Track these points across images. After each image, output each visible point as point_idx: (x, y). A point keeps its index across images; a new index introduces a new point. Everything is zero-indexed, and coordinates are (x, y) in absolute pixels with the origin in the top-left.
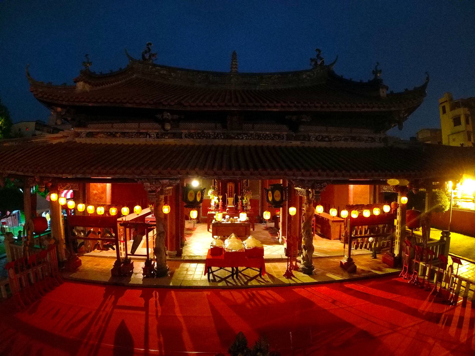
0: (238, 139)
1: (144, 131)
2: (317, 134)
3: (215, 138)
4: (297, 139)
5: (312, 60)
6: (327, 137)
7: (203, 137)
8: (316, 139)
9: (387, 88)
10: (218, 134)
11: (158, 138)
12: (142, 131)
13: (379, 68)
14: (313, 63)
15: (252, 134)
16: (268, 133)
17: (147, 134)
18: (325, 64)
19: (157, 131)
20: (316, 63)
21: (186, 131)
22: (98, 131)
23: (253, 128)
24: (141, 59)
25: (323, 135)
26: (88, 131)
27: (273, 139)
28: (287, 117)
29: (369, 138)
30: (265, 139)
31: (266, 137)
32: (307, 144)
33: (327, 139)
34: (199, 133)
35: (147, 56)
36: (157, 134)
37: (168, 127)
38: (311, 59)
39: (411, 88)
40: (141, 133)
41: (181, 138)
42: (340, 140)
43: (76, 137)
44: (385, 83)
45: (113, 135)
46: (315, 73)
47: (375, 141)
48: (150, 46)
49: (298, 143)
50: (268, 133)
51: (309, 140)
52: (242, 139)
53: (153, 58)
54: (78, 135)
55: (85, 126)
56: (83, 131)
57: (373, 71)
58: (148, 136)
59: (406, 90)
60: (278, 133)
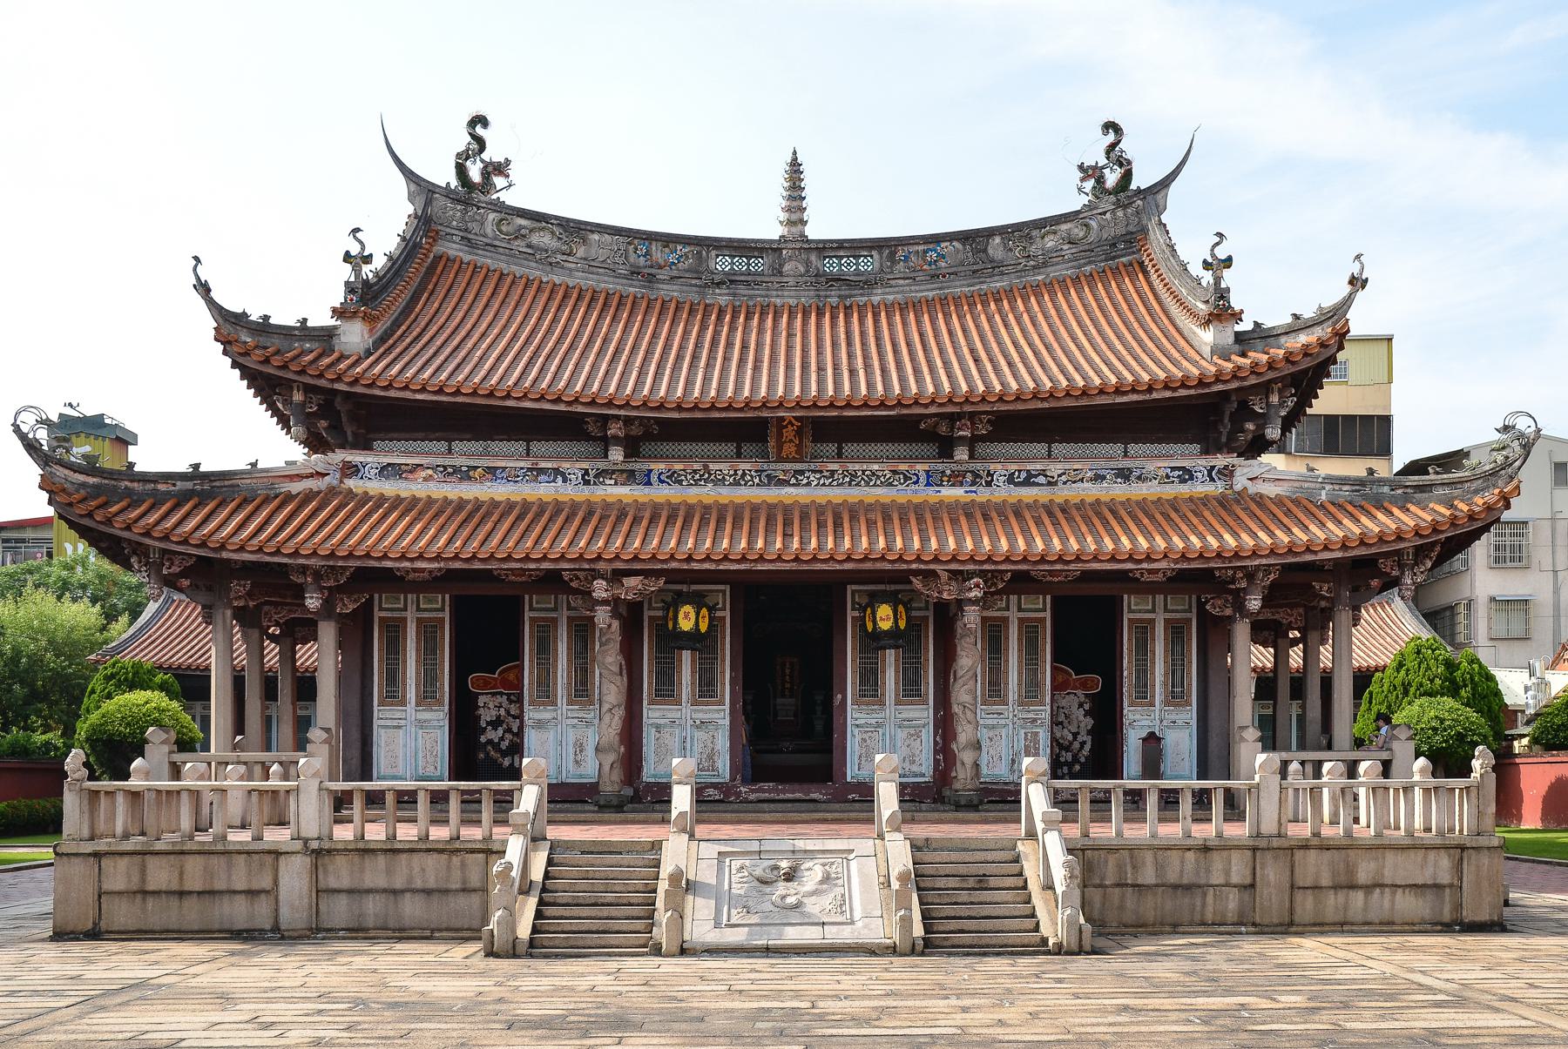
0: (797, 485)
1: (549, 465)
2: (1013, 467)
3: (736, 484)
4: (956, 479)
5: (1087, 171)
6: (1043, 473)
9: (1237, 316)
10: (744, 474)
11: (587, 483)
12: (543, 465)
13: (1221, 253)
14: (1089, 185)
15: (833, 472)
16: (876, 467)
17: (557, 471)
18: (1133, 186)
19: (585, 465)
20: (1100, 180)
21: (662, 466)
22: (417, 461)
23: (840, 455)
26: (386, 460)
27: (891, 484)
28: (923, 426)
29: (1173, 469)
30: (867, 484)
31: (871, 479)
32: (983, 495)
33: (1041, 479)
34: (695, 472)
36: (586, 472)
37: (616, 454)
38: (1081, 167)
39: (1308, 313)
40: (542, 471)
41: (649, 483)
42: (1082, 480)
43: (349, 476)
44: (1236, 302)
45: (465, 475)
46: (1093, 223)
49: (958, 492)
50: (876, 467)
51: (989, 484)
52: (809, 484)
54: (350, 470)
55: (366, 446)
56: (369, 459)
57: (1205, 261)
58: (560, 478)
59: (1296, 317)
60: (903, 467)
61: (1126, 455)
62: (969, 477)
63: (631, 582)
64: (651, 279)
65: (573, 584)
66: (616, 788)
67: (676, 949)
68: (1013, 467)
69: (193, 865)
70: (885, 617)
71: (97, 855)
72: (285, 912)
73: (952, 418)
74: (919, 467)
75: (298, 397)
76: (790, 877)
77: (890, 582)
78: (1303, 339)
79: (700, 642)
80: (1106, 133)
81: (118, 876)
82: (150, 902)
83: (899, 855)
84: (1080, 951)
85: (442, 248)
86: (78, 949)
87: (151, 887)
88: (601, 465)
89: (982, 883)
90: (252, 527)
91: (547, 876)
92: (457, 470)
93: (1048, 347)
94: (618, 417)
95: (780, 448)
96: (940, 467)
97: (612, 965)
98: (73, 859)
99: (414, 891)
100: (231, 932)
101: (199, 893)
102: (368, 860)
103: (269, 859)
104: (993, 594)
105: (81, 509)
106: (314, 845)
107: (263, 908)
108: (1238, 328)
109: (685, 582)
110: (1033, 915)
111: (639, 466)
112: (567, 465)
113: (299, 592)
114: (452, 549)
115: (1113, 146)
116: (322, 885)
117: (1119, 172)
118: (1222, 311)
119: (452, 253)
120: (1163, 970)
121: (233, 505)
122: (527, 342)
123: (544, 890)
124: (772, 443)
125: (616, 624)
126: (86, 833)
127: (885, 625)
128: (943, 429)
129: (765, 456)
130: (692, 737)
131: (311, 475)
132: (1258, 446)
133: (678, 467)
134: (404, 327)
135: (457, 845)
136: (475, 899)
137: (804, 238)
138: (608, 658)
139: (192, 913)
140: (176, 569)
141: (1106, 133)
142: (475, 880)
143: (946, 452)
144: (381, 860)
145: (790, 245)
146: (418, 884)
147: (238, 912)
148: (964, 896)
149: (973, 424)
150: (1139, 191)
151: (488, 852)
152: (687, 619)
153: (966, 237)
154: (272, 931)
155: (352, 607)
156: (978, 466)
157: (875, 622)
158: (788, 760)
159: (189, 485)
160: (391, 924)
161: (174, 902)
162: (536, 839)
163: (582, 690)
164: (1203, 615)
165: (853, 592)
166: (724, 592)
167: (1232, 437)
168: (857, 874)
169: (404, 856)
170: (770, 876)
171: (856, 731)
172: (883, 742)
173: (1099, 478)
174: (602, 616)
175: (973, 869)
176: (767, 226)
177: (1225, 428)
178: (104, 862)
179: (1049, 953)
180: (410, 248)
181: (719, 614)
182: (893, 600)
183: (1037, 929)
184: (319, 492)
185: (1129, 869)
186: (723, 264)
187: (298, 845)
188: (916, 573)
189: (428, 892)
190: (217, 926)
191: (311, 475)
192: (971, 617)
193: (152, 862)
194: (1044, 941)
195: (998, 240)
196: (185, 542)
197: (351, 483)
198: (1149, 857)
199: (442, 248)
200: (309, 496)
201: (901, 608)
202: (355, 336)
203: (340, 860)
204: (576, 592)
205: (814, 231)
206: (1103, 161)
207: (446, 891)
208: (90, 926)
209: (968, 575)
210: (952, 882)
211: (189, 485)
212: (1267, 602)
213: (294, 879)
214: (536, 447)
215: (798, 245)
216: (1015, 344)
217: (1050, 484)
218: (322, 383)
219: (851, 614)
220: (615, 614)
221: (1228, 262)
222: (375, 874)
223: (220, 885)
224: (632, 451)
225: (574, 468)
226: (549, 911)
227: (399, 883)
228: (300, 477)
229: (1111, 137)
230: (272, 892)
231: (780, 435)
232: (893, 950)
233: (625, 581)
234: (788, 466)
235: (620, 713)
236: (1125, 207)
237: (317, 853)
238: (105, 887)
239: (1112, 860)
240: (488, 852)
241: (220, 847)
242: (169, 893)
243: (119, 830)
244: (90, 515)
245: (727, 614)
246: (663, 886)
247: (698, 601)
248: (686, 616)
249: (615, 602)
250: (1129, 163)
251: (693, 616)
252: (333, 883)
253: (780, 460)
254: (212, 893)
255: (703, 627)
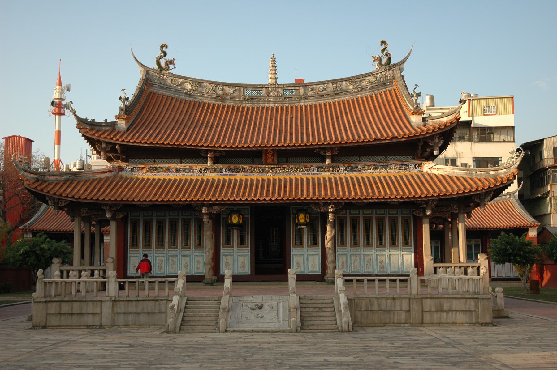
3: (252, 172)
7: (242, 171)
8: (346, 170)
9: (422, 113)
11: (201, 173)
13: (417, 91)
14: (377, 63)
18: (392, 63)
20: (380, 60)
21: (226, 166)
24: (156, 67)
25: (353, 165)
28: (315, 151)
30: (296, 172)
33: (356, 169)
35: (163, 63)
36: (201, 169)
43: (121, 171)
47: (409, 168)
48: (164, 49)
53: (171, 66)
60: (309, 166)
61: (386, 160)
62: (331, 169)
63: (216, 207)
64: (223, 100)
65: (197, 208)
66: (211, 277)
67: (224, 330)
68: (346, 165)
69: (76, 305)
70: (302, 218)
71: (46, 302)
72: (104, 320)
73: (324, 149)
74: (314, 165)
75: (103, 146)
76: (261, 307)
77: (304, 206)
78: (445, 120)
79: (241, 227)
80: (382, 44)
81: (53, 308)
82: (62, 316)
83: (294, 300)
84: (349, 331)
85: (151, 89)
86: (42, 331)
87: (62, 312)
88: (205, 167)
89: (321, 309)
90: (89, 191)
91: (186, 308)
92: (156, 169)
93: (359, 123)
94: (211, 151)
95: (266, 160)
96: (321, 165)
97: (204, 335)
98: (39, 304)
99: (144, 313)
100: (87, 326)
101: (77, 314)
102: (130, 303)
103: (99, 303)
104: (339, 209)
105: (33, 186)
106: (113, 299)
107: (97, 319)
108: (423, 116)
109: (234, 207)
110: (336, 320)
111: (219, 166)
112: (194, 167)
113: (104, 211)
114: (156, 198)
115: (384, 49)
116: (115, 311)
117: (386, 58)
118: (418, 111)
119: (155, 91)
120: (369, 337)
121: (82, 183)
122: (181, 124)
123: (185, 312)
124: (264, 159)
125: (211, 221)
126: (43, 295)
127: (302, 221)
128: (322, 153)
129: (261, 163)
130: (238, 259)
131: (108, 172)
132: (431, 158)
133: (232, 167)
134: (139, 120)
135: (158, 298)
136: (163, 315)
137: (276, 83)
138: (208, 234)
139: (75, 320)
140: (63, 205)
141: (382, 44)
142: (163, 310)
143: (324, 161)
144: (134, 303)
145: (272, 86)
146: (145, 311)
147: (89, 320)
148: (314, 314)
149: (332, 151)
150: (394, 65)
151: (167, 300)
152: (235, 220)
153: (334, 82)
154: (100, 326)
155: (121, 216)
156: (335, 165)
157: (298, 220)
158: (270, 266)
159: (68, 176)
160: (137, 323)
161: (70, 317)
162: (181, 296)
163: (200, 243)
164: (414, 216)
165: (293, 208)
166: (248, 209)
167: (422, 154)
168: (276, 307)
169: (141, 302)
170: (254, 307)
171: (294, 256)
172: (304, 259)
173: (375, 169)
174: (205, 218)
175: (318, 305)
176: (265, 79)
177: (420, 151)
178: (49, 304)
179: (339, 331)
180: (141, 92)
181: (246, 216)
182: (305, 212)
183: (336, 324)
184: (111, 177)
185: (369, 305)
186: (249, 93)
187: (108, 299)
188: (312, 203)
189: (148, 313)
190: (83, 324)
191: (108, 172)
192: (331, 217)
193: (63, 305)
194: (338, 328)
195: (344, 83)
196: (67, 196)
197: (122, 173)
198: (376, 301)
199: (151, 89)
200: (108, 178)
201: (307, 215)
202: (122, 124)
203: (121, 303)
204: (197, 211)
205: (279, 82)
206: (381, 55)
207: (154, 313)
208: (44, 324)
209: (329, 204)
210: (311, 309)
211: (68, 176)
212: (433, 211)
213: (107, 309)
214: (183, 160)
215: (275, 86)
216: (348, 122)
217: (360, 171)
218: (112, 141)
219: (292, 216)
220: (210, 218)
221: (419, 95)
222: (132, 308)
223: (84, 311)
224: (216, 161)
225: (197, 167)
226: (186, 319)
227: (139, 311)
228: (104, 172)
229: (383, 46)
230: (100, 314)
231: (266, 156)
232: (290, 331)
233: (213, 207)
234: (269, 166)
235: (212, 251)
236: (389, 70)
237: (115, 301)
238: (49, 312)
239: (364, 302)
240: (167, 300)
241: (84, 299)
242: (68, 314)
243: (53, 293)
244: (36, 188)
245: (249, 216)
246: (221, 311)
247: (239, 212)
248: (235, 218)
249: (210, 215)
250: (390, 54)
251: (237, 218)
252: (119, 311)
253: (266, 163)
254: (81, 314)
255: (241, 222)
